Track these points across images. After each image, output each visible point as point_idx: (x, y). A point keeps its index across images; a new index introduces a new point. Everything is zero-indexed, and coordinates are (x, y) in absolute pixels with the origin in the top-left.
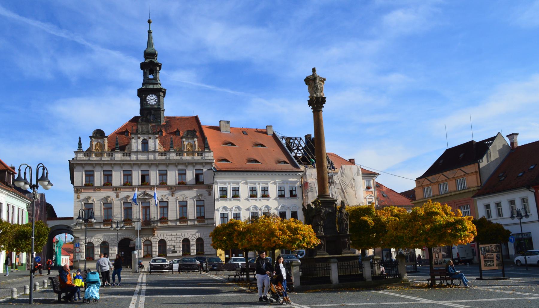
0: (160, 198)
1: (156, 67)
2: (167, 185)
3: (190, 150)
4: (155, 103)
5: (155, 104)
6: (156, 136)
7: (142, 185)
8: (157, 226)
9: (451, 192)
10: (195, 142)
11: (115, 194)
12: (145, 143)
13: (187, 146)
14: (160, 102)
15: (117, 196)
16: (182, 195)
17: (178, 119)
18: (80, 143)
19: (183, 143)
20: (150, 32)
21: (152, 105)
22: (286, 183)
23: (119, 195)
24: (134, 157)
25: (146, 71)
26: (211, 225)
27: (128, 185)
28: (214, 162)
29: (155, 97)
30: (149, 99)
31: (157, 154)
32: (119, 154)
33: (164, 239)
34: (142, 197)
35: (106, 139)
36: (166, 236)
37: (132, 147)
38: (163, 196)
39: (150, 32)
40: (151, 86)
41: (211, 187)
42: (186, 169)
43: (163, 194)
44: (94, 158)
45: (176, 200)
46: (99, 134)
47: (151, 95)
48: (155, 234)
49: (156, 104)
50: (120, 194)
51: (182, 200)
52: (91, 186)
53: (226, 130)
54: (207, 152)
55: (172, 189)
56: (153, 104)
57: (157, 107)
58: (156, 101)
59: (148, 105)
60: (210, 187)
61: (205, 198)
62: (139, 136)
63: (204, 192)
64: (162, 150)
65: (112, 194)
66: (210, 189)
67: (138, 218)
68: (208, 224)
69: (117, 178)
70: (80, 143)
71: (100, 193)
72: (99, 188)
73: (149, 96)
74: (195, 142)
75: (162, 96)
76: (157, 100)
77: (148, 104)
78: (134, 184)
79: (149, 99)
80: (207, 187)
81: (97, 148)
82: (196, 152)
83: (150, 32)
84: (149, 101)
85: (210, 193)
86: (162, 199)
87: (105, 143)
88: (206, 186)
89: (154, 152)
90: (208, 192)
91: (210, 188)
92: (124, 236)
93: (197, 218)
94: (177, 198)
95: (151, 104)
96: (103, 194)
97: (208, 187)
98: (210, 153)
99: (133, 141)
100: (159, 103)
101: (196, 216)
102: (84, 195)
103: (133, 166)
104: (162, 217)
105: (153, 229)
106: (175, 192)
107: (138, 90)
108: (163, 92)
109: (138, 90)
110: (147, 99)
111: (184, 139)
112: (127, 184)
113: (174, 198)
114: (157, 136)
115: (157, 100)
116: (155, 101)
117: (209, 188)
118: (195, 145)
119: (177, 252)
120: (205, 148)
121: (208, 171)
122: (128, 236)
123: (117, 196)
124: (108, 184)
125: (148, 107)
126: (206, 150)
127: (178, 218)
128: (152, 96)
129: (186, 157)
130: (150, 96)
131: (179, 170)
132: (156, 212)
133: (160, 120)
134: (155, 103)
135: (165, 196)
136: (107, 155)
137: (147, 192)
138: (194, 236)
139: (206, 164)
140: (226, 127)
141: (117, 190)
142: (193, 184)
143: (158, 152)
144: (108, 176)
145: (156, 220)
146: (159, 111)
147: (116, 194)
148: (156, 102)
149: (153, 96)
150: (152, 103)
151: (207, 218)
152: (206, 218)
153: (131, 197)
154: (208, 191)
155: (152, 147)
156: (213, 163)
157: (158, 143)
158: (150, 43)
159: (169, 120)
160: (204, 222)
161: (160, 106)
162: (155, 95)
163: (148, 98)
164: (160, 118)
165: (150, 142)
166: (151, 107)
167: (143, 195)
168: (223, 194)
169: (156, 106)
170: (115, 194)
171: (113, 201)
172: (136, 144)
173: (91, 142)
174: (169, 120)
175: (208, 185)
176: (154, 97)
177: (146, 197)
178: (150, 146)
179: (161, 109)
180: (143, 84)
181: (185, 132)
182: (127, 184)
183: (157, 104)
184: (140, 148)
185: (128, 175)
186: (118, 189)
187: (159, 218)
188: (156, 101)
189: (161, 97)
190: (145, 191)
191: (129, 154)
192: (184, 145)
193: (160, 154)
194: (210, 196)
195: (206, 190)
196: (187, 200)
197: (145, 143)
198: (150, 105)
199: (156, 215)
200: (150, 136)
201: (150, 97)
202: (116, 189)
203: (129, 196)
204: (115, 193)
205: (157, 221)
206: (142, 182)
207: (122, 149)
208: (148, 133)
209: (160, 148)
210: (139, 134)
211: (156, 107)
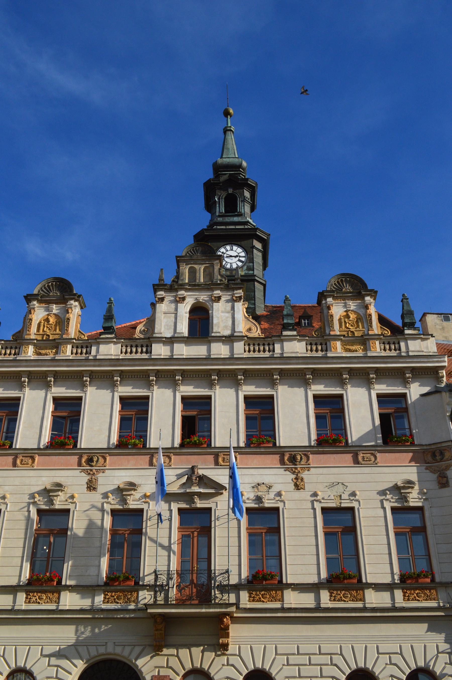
0: (252, 496)
1: (243, 191)
2: (275, 444)
3: (352, 332)
4: (240, 264)
6: (235, 292)
7: (182, 445)
8: (237, 604)
10: (367, 307)
11: (85, 478)
13: (340, 320)
14: (253, 263)
16: (332, 485)
19: (325, 311)
20: (228, 128)
23: (96, 480)
25: (216, 199)
27: (135, 446)
28: (446, 364)
29: (239, 250)
32: (112, 345)
33: (267, 667)
34: (182, 491)
35: (77, 303)
36: (276, 654)
37: (156, 326)
38: (263, 488)
43: (260, 481)
45: (312, 502)
47: (228, 247)
48: (227, 645)
49: (242, 267)
51: (334, 505)
52: (6, 449)
53: (446, 337)
54: (414, 337)
55: (293, 460)
56: (234, 266)
58: (243, 259)
60: (442, 454)
62: (182, 293)
64: (256, 333)
66: (441, 460)
67: (162, 568)
71: (32, 473)
73: (222, 250)
74: (368, 309)
75: (257, 249)
76: (245, 257)
78: (153, 442)
80: (429, 458)
81: (43, 331)
82: (376, 337)
85: (447, 477)
86: (259, 499)
87: (71, 316)
88: (424, 452)
90: (434, 477)
92: (102, 650)
93: (403, 578)
94: (315, 494)
98: (425, 342)
99: (162, 308)
100: (251, 264)
101: (396, 570)
104: (258, 572)
105: (220, 617)
106: (306, 472)
107: (194, 236)
108: (260, 239)
109: (194, 236)
111: (330, 300)
113: (305, 495)
114: (240, 293)
115: (245, 257)
116: (239, 260)
117: (438, 458)
118: (370, 315)
121: (424, 398)
122: (118, 650)
127: (324, 575)
128: (232, 250)
130: (225, 248)
132: (234, 551)
133: (255, 304)
135: (270, 487)
137: (201, 472)
138: (396, 659)
140: (443, 328)
141: (94, 464)
143: (240, 338)
145: (234, 580)
146: (252, 283)
147: (89, 477)
149: (235, 248)
150: (231, 266)
151: (444, 580)
153: (139, 489)
154: (433, 472)
155: (222, 325)
156: (443, 368)
157: (241, 312)
158: (228, 149)
161: (253, 271)
164: (255, 300)
165: (218, 310)
167: (184, 479)
169: (242, 271)
170: (85, 478)
171: (75, 503)
175: (433, 447)
176: (237, 250)
177: (196, 489)
178: (215, 321)
179: (256, 278)
181: (333, 280)
183: (245, 268)
186: (95, 459)
187: (245, 574)
189: (255, 251)
190: (193, 468)
192: (332, 316)
193: (249, 345)
194: (446, 491)
195: (427, 469)
196: (355, 504)
198: (227, 270)
199: (234, 561)
200: (217, 293)
201: (227, 251)
202: (90, 461)
203: (132, 486)
204: (83, 474)
205: (237, 588)
206: (184, 436)
209: (249, 330)
210: (182, 287)
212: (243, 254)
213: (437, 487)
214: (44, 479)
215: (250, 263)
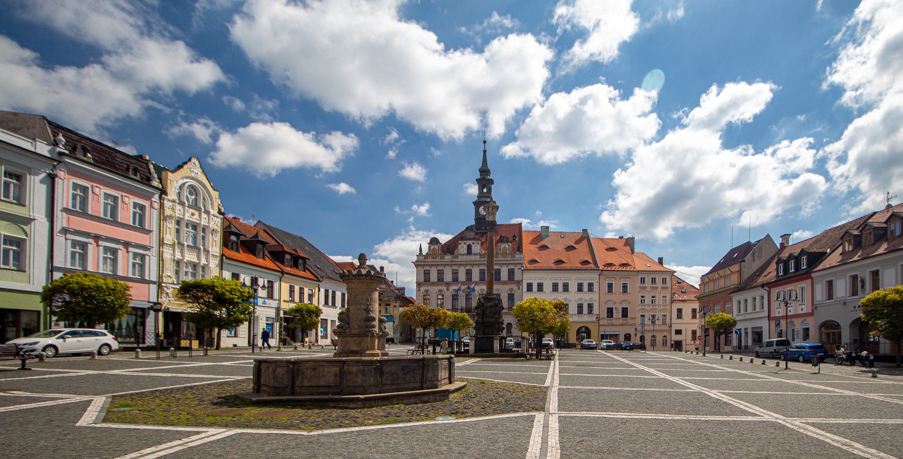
9: (721, 288)
12: (469, 247)
15: (448, 290)
18: (421, 249)
31: (479, 256)
39: (485, 151)
40: (483, 199)
44: (430, 259)
62: (465, 242)
63: (515, 287)
65: (444, 288)
70: (421, 249)
72: (433, 284)
83: (485, 151)
89: (476, 254)
91: (519, 283)
96: (436, 288)
102: (423, 289)
120: (519, 251)
123: (448, 290)
124: (440, 280)
144: (440, 273)
168: (530, 287)
172: (462, 248)
173: (430, 247)
182: (455, 280)
184: (466, 252)
185: (455, 273)
191: (457, 257)
197: (469, 247)
200: (474, 242)
207: (452, 253)
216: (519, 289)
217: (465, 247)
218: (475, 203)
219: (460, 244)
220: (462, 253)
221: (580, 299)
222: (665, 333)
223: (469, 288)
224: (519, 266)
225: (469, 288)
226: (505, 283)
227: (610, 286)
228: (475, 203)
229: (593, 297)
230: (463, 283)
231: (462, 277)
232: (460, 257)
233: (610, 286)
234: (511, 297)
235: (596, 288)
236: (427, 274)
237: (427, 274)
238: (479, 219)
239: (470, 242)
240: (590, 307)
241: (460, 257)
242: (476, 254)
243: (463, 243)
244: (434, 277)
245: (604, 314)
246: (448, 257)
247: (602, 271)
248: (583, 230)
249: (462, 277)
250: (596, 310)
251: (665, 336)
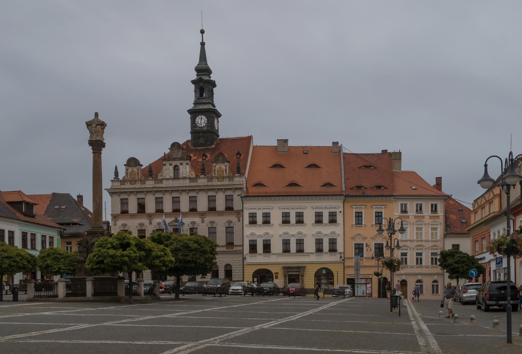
5: (204, 126)
15: (151, 223)
17: (229, 141)
21: (201, 127)
22: (292, 208)
24: (165, 184)
26: (239, 252)
30: (198, 121)
31: (188, 181)
40: (201, 107)
41: (240, 213)
42: (216, 195)
46: (133, 162)
49: (205, 126)
50: (153, 221)
54: (237, 176)
56: (202, 126)
57: (207, 129)
58: (206, 122)
59: (197, 128)
60: (239, 213)
61: (234, 225)
63: (233, 218)
68: (236, 251)
69: (151, 207)
72: (133, 216)
77: (197, 127)
79: (198, 121)
84: (198, 122)
89: (184, 178)
90: (237, 219)
91: (239, 213)
95: (200, 126)
97: (238, 213)
103: (207, 191)
106: (205, 218)
110: (196, 121)
112: (159, 211)
113: (205, 224)
119: (206, 278)
120: (238, 172)
125: (198, 130)
126: (236, 175)
129: (215, 182)
131: (139, 198)
134: (204, 124)
136: (141, 183)
139: (236, 189)
142: (223, 210)
148: (205, 123)
149: (203, 117)
152: (234, 244)
159: (220, 142)
160: (233, 249)
162: (204, 115)
163: (197, 120)
166: (200, 129)
172: (168, 171)
174: (220, 142)
180: (195, 104)
183: (206, 126)
185: (159, 201)
188: (206, 122)
191: (161, 181)
198: (200, 127)
204: (148, 220)
208: (180, 159)
211: (205, 129)
212: (206, 120)
213: (238, 221)
214: (138, 221)
215: (208, 124)
216: (239, 221)
217: (171, 168)
218: (190, 112)
219: (165, 165)
220: (168, 177)
221: (319, 233)
222: (436, 277)
223: (176, 221)
224: (239, 192)
225: (176, 221)
226: (221, 214)
227: (359, 216)
228: (190, 112)
229: (337, 230)
230: (168, 215)
231: (168, 207)
232: (164, 182)
233: (359, 216)
234: (229, 231)
235: (339, 218)
236: (124, 202)
237: (124, 202)
238: (195, 131)
239: (177, 163)
240: (333, 242)
241: (164, 182)
242: (184, 178)
243: (168, 163)
244: (133, 208)
245: (351, 252)
246: (150, 184)
247: (346, 196)
248: (333, 143)
249: (168, 207)
250: (340, 247)
251: (435, 281)
